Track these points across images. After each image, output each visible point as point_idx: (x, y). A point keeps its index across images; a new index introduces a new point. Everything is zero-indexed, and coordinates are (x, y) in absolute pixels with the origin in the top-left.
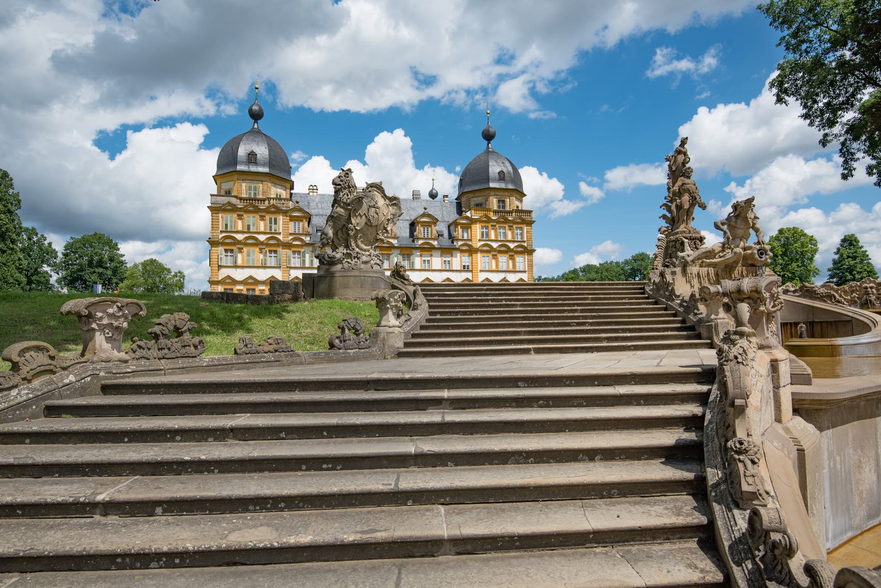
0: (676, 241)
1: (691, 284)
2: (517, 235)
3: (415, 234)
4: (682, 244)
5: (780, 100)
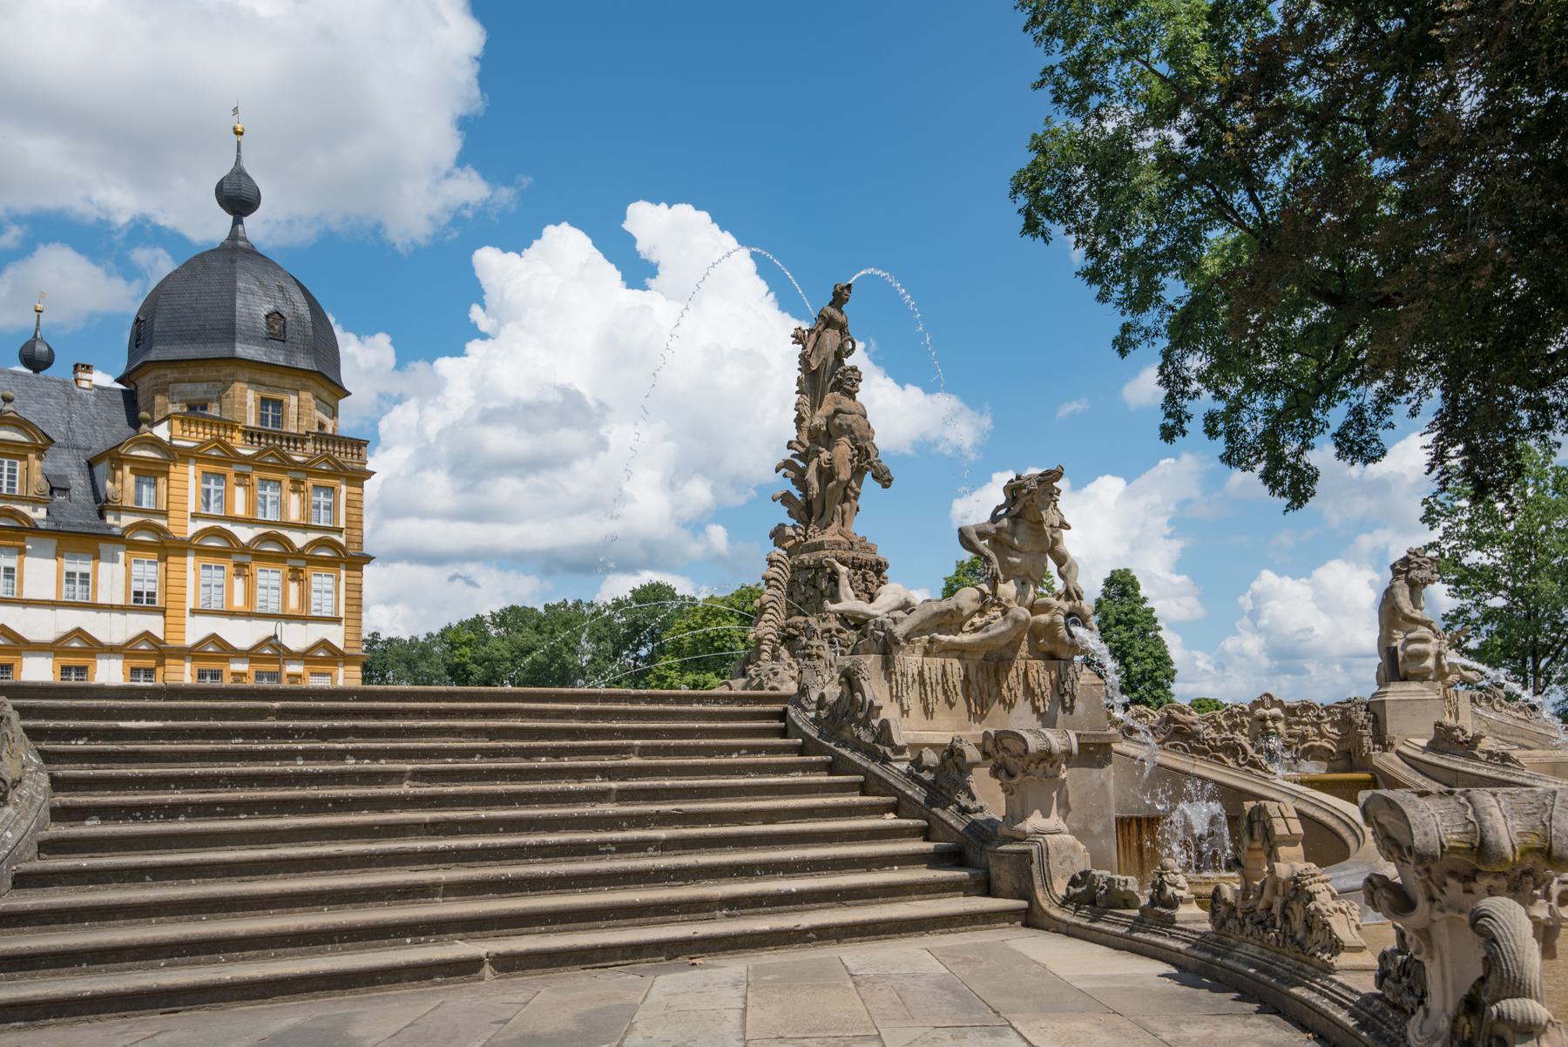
0: (819, 567)
1: (902, 705)
2: (317, 507)
4: (834, 578)
5: (1031, 227)
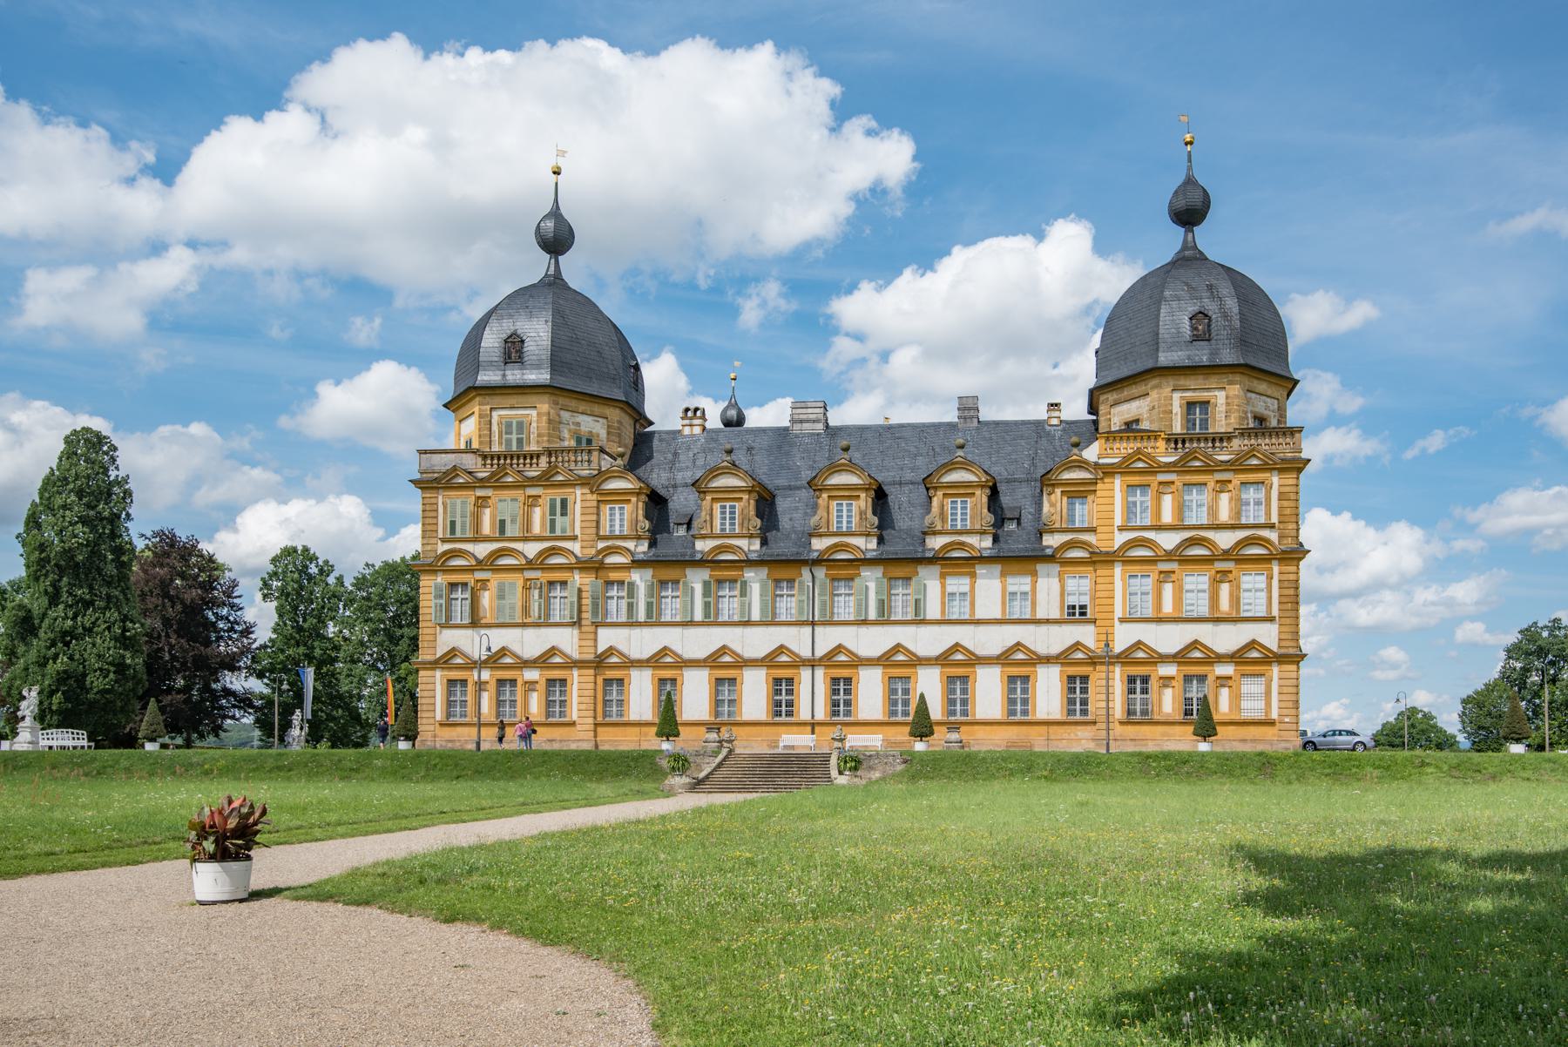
2: (1249, 504)
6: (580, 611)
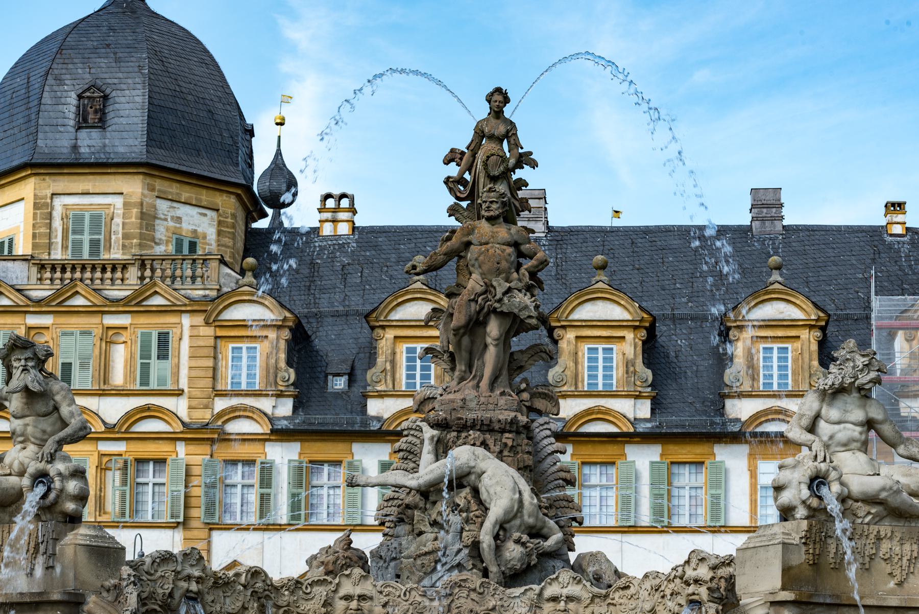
3: (729, 375)
6: (187, 507)
